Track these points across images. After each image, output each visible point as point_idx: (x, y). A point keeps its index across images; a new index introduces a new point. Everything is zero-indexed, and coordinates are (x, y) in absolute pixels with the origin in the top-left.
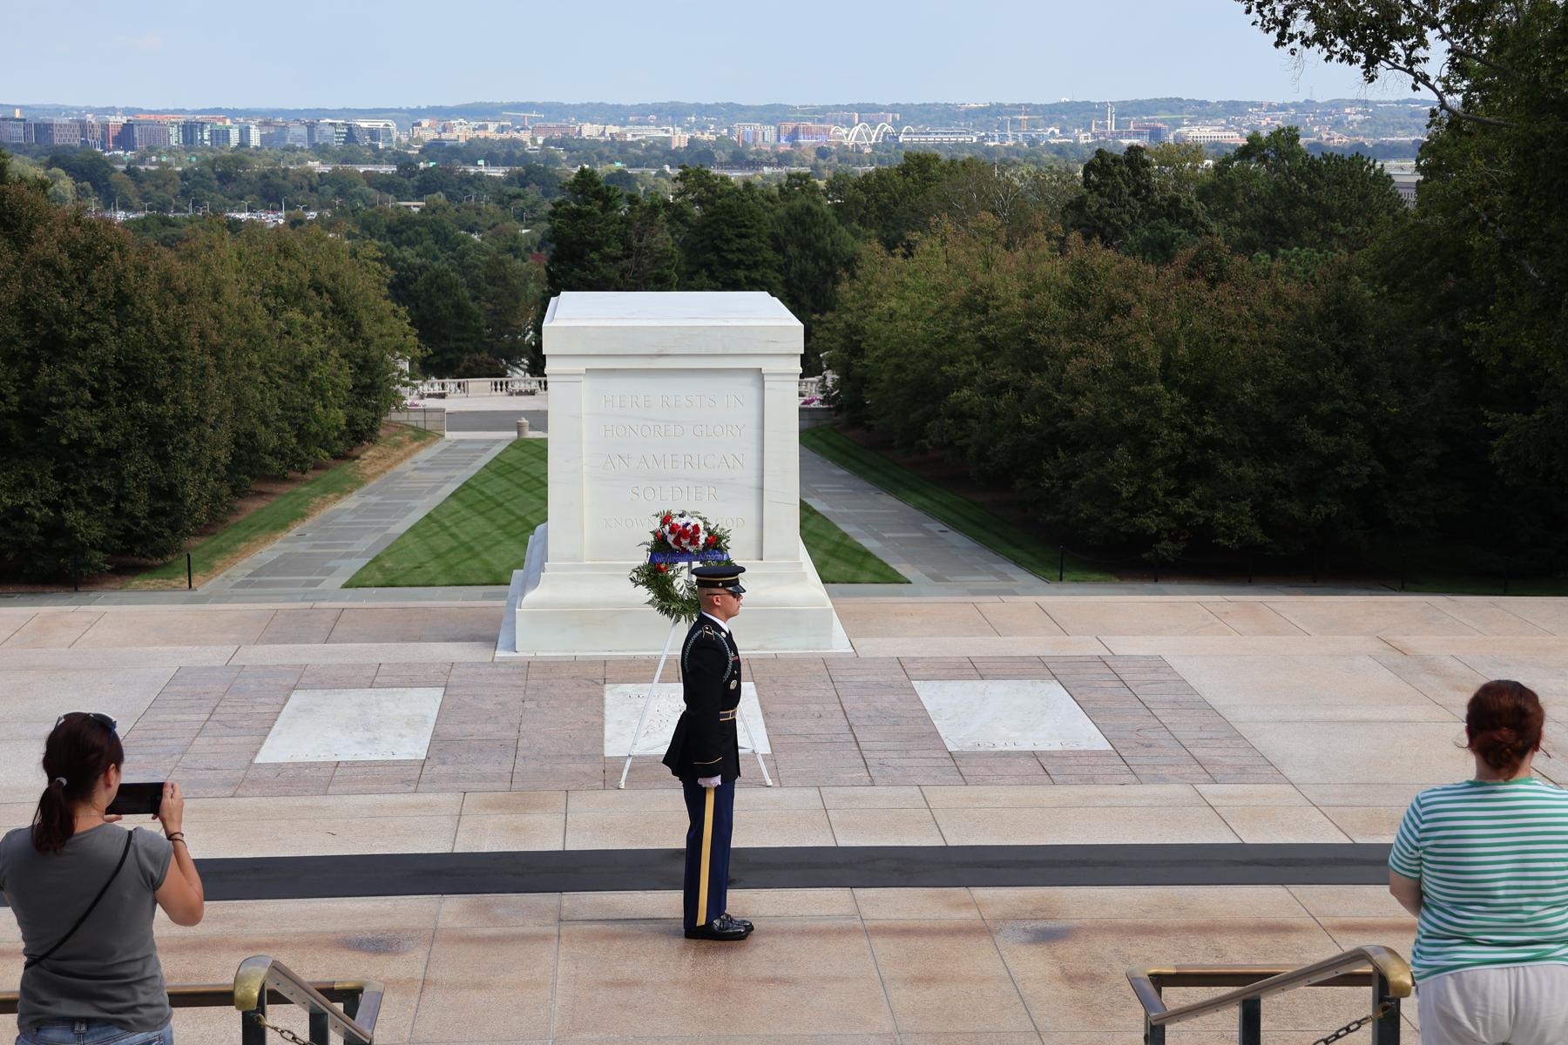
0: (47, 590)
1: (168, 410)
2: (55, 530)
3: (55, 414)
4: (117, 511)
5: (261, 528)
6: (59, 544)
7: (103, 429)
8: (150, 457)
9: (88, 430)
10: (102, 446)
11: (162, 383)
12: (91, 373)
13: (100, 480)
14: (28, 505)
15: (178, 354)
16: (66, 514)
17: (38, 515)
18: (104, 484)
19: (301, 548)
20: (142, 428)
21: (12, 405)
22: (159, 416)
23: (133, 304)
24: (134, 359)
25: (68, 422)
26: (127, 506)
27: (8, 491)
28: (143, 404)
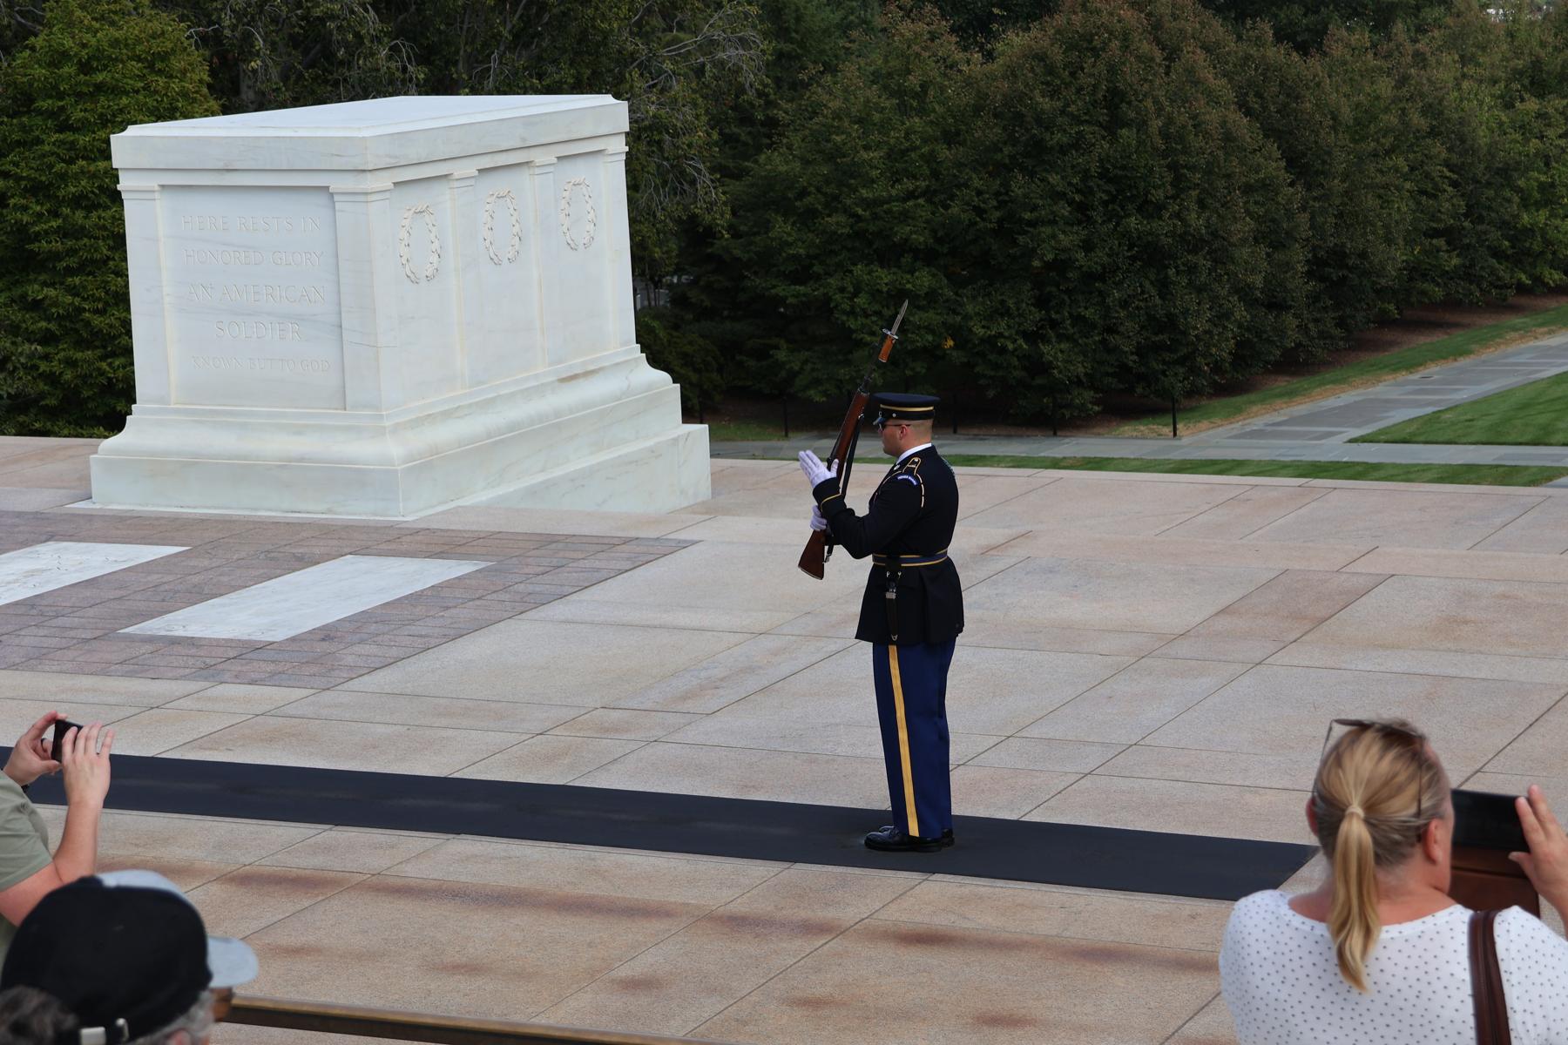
0: (1028, 433)
1: (1163, 227)
2: (1037, 366)
3: (1028, 232)
4: (1103, 341)
5: (1385, 367)
6: (1039, 381)
7: (1088, 246)
8: (1152, 283)
9: (1064, 250)
10: (1084, 269)
11: (1158, 195)
12: (1070, 184)
13: (1086, 308)
14: (1001, 335)
15: (1182, 159)
16: (1045, 348)
17: (1011, 347)
18: (1087, 313)
19: (1394, 393)
20: (1130, 249)
21: (990, 222)
22: (1150, 234)
23: (1129, 103)
24: (1124, 168)
25: (1044, 242)
26: (1114, 340)
27: (985, 319)
28: (1133, 222)
